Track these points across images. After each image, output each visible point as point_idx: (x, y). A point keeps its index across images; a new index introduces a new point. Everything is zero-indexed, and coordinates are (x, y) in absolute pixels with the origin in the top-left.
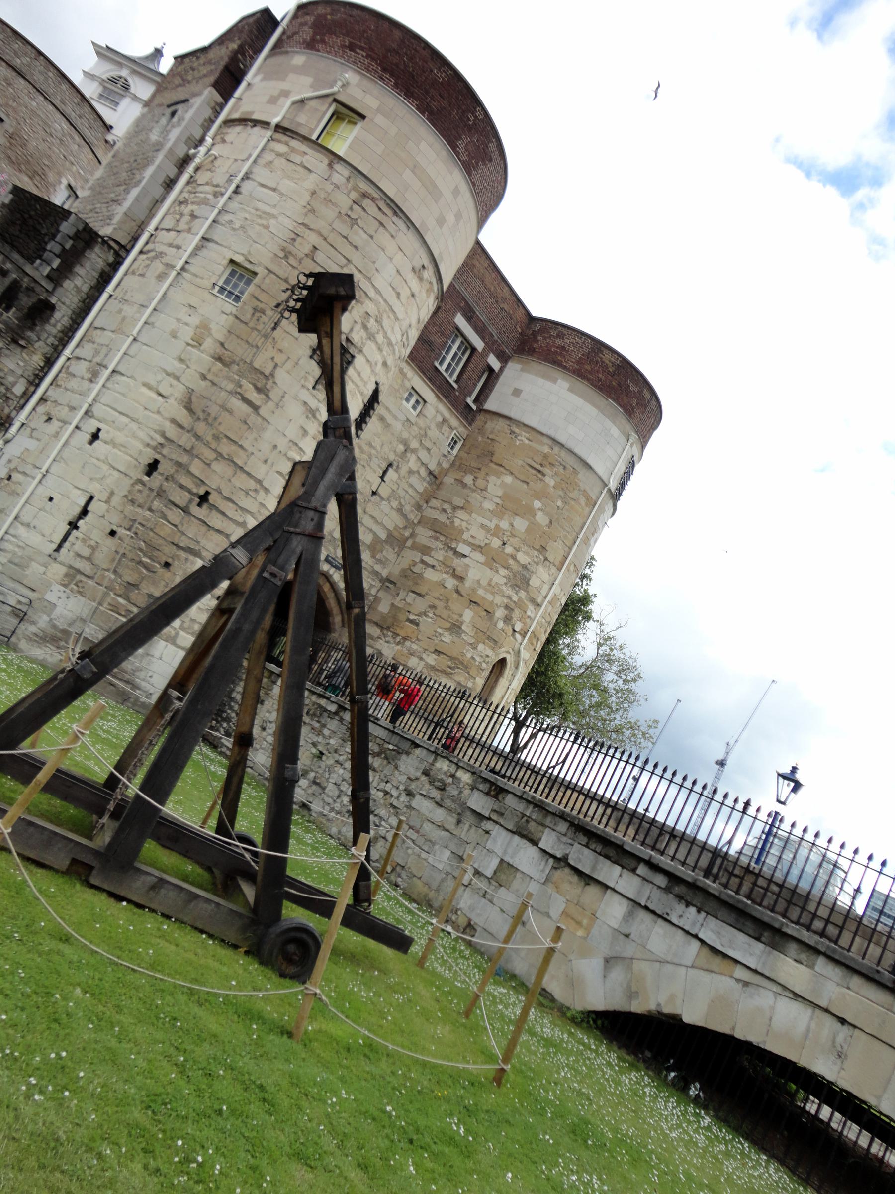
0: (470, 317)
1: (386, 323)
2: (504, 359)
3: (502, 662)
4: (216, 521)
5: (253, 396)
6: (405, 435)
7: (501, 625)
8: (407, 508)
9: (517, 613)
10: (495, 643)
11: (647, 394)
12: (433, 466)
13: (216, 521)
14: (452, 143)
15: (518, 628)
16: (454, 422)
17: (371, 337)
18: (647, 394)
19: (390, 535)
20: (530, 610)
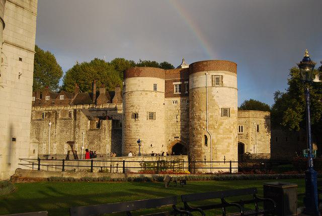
0: (175, 81)
1: (140, 105)
2: (188, 80)
3: (206, 137)
4: (133, 147)
5: (129, 129)
6: (176, 109)
7: (200, 129)
8: (186, 119)
9: (202, 125)
10: (201, 134)
11: (204, 63)
12: (186, 109)
13: (133, 147)
14: (134, 77)
15: (204, 127)
16: (185, 99)
17: (139, 109)
18: (205, 63)
19: (185, 126)
20: (205, 123)
